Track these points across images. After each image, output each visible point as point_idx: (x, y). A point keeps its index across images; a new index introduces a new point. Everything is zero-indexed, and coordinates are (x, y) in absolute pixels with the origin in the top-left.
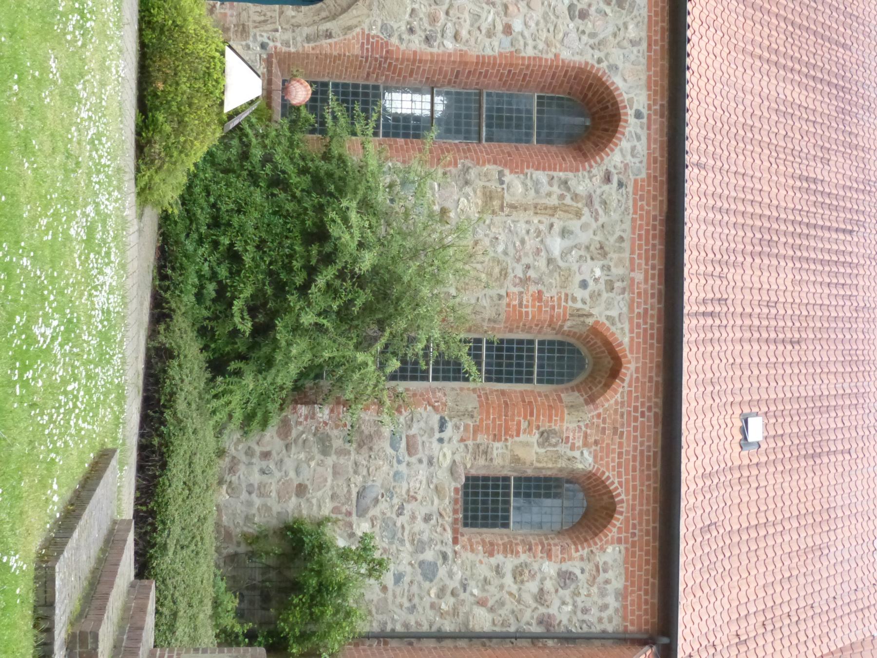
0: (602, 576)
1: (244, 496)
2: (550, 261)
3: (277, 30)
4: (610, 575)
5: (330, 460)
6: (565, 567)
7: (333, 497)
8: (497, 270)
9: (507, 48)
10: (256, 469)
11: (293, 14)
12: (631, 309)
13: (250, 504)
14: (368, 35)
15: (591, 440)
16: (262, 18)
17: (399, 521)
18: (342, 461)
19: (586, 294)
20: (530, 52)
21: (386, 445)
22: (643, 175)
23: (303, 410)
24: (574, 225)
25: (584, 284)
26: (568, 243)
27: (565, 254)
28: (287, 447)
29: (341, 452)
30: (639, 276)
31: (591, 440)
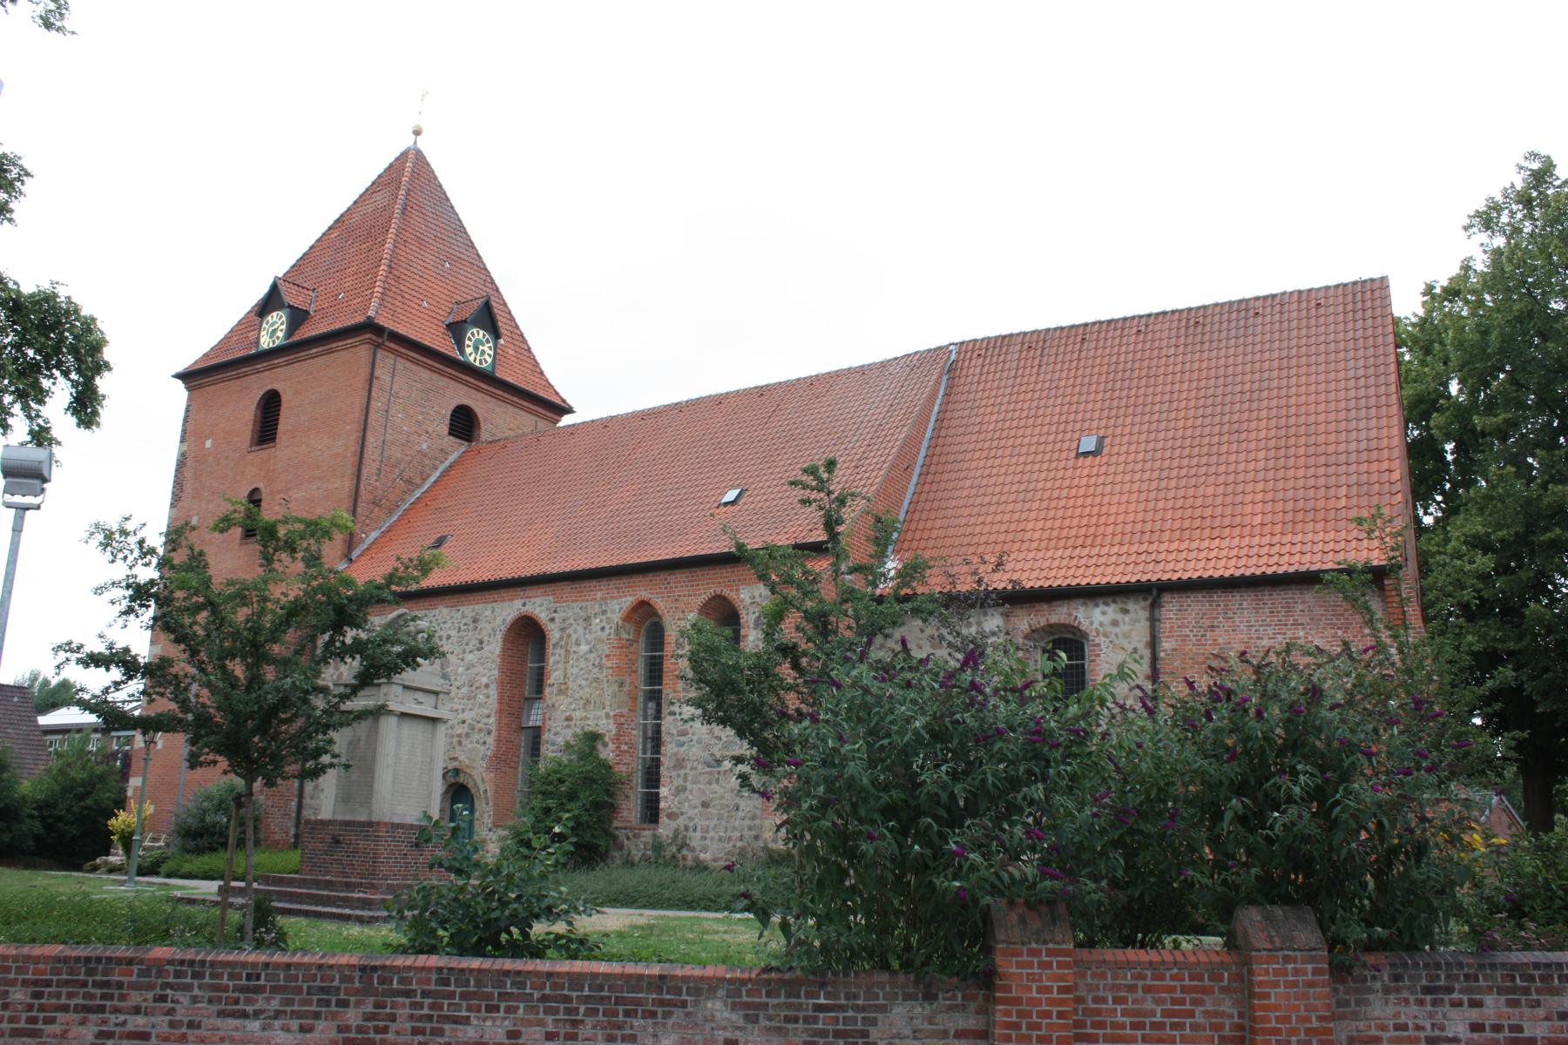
0: (758, 599)
1: (708, 842)
2: (591, 652)
4: (757, 594)
5: (689, 786)
6: (752, 625)
7: (710, 783)
8: (595, 684)
9: (493, 686)
10: (693, 834)
12: (613, 598)
13: (712, 839)
15: (681, 615)
17: (724, 739)
18: (690, 778)
19: (607, 627)
20: (496, 672)
21: (682, 749)
22: (551, 598)
23: (662, 805)
24: (574, 637)
25: (603, 629)
26: (583, 642)
27: (588, 643)
28: (682, 814)
29: (685, 780)
30: (599, 595)
31: (681, 615)
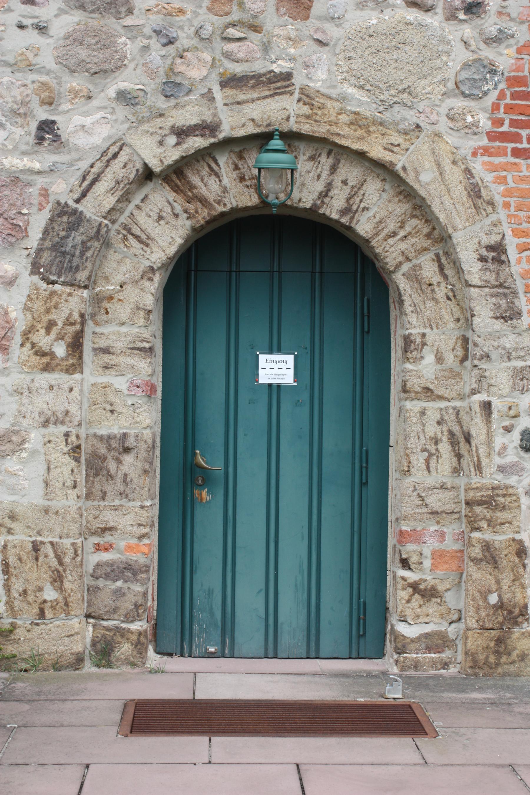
3: (487, 406)
11: (429, 358)
14: (491, 136)
16: (445, 447)
